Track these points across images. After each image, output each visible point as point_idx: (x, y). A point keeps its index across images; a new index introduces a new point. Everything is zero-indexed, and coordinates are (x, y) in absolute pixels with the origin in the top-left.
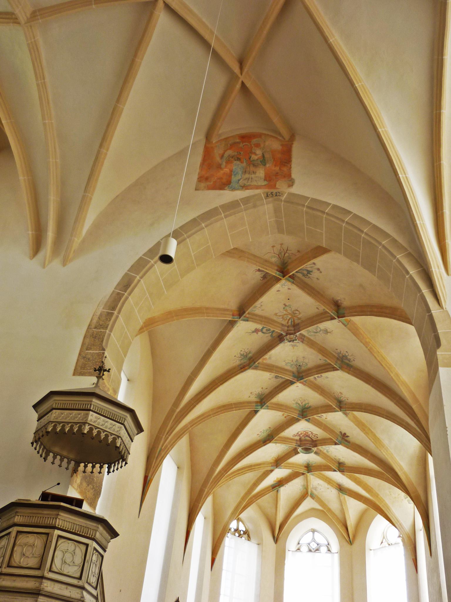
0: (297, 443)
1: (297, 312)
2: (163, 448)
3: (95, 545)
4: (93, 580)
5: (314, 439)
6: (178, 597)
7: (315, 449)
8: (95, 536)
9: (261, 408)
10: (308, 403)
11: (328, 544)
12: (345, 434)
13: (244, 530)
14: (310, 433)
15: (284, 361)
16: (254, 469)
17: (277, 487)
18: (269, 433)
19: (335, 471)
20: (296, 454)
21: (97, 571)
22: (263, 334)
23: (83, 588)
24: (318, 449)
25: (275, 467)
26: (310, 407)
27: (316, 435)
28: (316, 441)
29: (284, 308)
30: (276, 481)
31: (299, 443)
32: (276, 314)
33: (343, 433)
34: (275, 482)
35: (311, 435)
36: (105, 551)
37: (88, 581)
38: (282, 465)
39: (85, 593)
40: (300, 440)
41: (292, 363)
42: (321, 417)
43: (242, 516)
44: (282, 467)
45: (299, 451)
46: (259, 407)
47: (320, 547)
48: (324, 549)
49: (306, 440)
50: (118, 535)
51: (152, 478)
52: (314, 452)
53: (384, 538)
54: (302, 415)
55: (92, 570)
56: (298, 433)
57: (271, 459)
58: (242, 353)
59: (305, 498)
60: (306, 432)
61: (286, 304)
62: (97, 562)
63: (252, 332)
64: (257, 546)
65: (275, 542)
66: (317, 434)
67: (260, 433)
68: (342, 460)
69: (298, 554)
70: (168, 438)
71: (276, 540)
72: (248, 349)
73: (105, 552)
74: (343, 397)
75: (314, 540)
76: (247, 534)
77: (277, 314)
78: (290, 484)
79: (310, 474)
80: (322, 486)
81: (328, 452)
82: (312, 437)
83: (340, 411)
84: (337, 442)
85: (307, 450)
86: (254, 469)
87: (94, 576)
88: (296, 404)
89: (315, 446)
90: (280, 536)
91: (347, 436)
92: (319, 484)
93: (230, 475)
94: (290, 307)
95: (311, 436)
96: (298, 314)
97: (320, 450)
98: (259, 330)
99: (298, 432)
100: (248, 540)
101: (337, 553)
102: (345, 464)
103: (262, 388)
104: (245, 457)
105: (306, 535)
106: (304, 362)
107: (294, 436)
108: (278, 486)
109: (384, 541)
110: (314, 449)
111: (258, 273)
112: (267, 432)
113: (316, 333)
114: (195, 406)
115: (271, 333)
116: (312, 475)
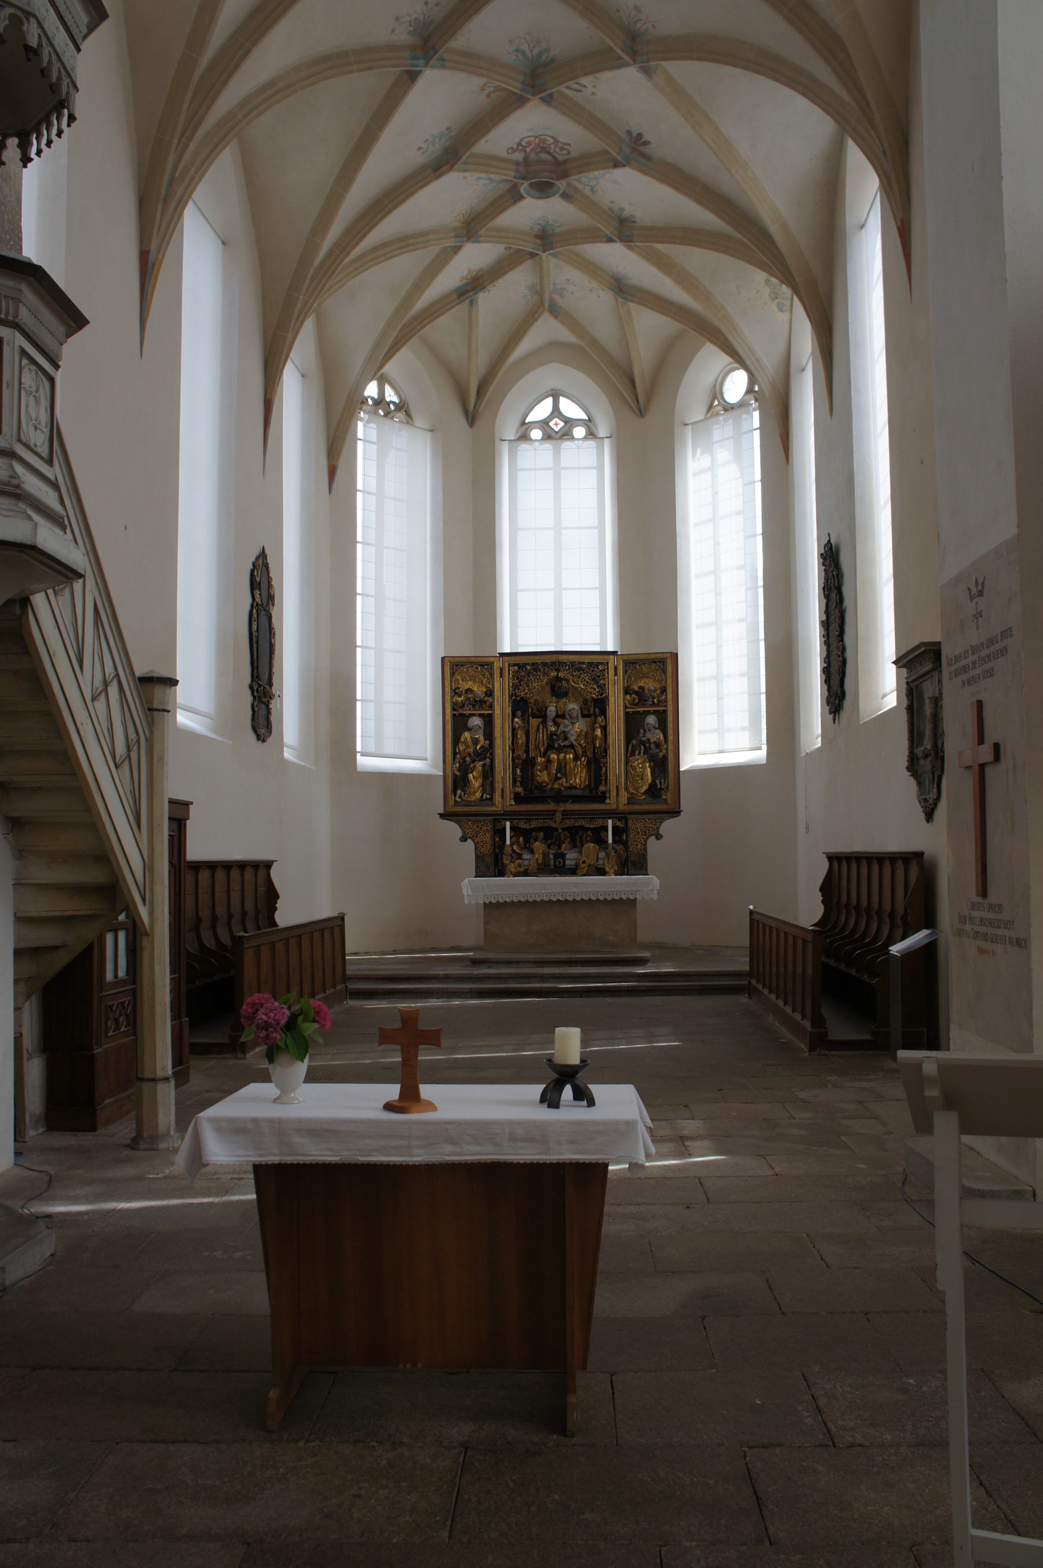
0: (517, 171)
2: (177, 174)
3: (21, 341)
4: (39, 439)
5: (561, 158)
6: (263, 547)
7: (562, 185)
8: (16, 316)
9: (426, 64)
10: (548, 50)
11: (590, 420)
12: (640, 136)
13: (396, 400)
14: (551, 141)
16: (413, 244)
17: (471, 293)
18: (448, 144)
19: (610, 240)
20: (515, 202)
21: (44, 418)
23: (11, 455)
24: (569, 185)
25: (465, 239)
26: (553, 61)
27: (565, 147)
28: (565, 162)
30: (467, 279)
31: (522, 169)
33: (634, 134)
34: (465, 281)
35: (553, 146)
36: (57, 367)
37: (23, 438)
38: (482, 232)
39: (19, 469)
40: (526, 162)
42: (581, 91)
43: (389, 369)
44: (482, 239)
45: (522, 191)
46: (421, 62)
47: (570, 427)
48: (579, 432)
49: (541, 162)
50: (87, 322)
51: (160, 256)
52: (561, 192)
53: (714, 397)
54: (533, 87)
55: (27, 411)
56: (519, 144)
59: (536, 316)
60: (540, 139)
62: (37, 391)
64: (429, 434)
65: (470, 424)
66: (568, 142)
67: (424, 146)
68: (629, 210)
69: (524, 446)
70: (187, 146)
71: (471, 417)
73: (57, 370)
74: (641, 20)
75: (556, 412)
76: (403, 410)
78: (501, 283)
79: (549, 254)
80: (575, 286)
81: (594, 194)
82: (555, 151)
83: (630, 61)
84: (619, 158)
85: (543, 189)
86: (413, 244)
87: (36, 428)
88: (516, 54)
89: (565, 175)
90: (480, 410)
91: (646, 143)
92: (568, 280)
93: (353, 262)
95: (552, 150)
97: (576, 189)
99: (522, 139)
100: (408, 423)
101: (610, 437)
102: (635, 222)
104: (390, 212)
105: (539, 405)
107: (510, 151)
108: (473, 289)
109: (716, 403)
110: (560, 186)
112: (443, 141)
114: (249, 51)
116: (555, 256)
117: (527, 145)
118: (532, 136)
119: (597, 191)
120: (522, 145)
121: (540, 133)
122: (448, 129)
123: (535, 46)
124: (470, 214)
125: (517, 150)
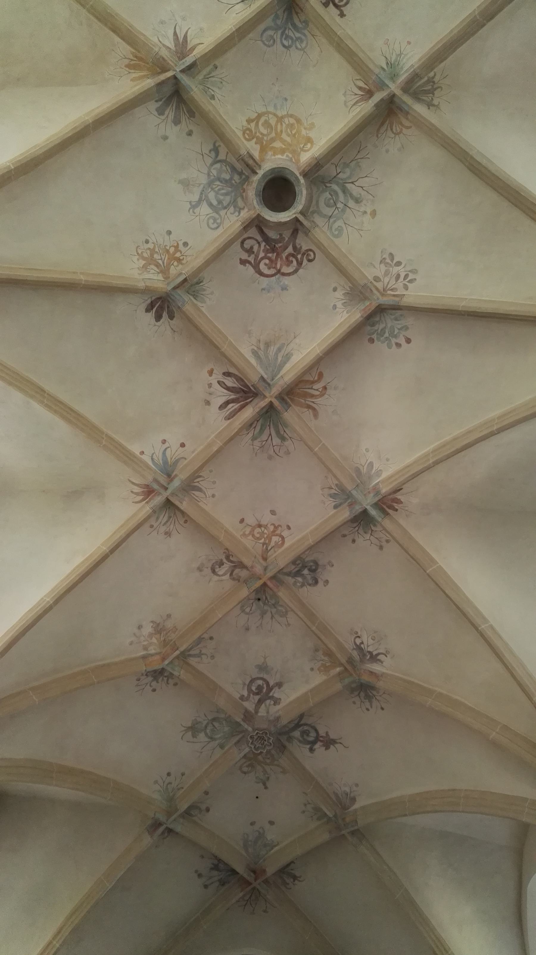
1: (245, 769)
10: (254, 439)
12: (158, 318)
15: (289, 625)
22: (318, 727)
29: (268, 778)
32: (284, 772)
35: (262, 255)
41: (274, 610)
56: (300, 264)
57: (405, 131)
58: (368, 705)
61: (263, 787)
63: (336, 743)
72: (354, 703)
77: (281, 772)
88: (285, 435)
91: (148, 310)
94: (256, 778)
95: (263, 244)
96: (245, 765)
98: (321, 741)
103: (354, 541)
106: (248, 614)
111: (297, 874)
112: (382, 326)
113: (214, 719)
115: (302, 722)
117: (291, 258)
118: (284, 274)
119: (210, 151)
120: (297, 260)
121: (273, 278)
122: (371, 341)
123: (266, 441)
124: (382, 124)
125: (303, 254)
